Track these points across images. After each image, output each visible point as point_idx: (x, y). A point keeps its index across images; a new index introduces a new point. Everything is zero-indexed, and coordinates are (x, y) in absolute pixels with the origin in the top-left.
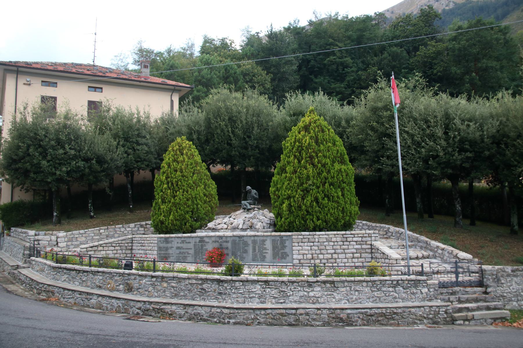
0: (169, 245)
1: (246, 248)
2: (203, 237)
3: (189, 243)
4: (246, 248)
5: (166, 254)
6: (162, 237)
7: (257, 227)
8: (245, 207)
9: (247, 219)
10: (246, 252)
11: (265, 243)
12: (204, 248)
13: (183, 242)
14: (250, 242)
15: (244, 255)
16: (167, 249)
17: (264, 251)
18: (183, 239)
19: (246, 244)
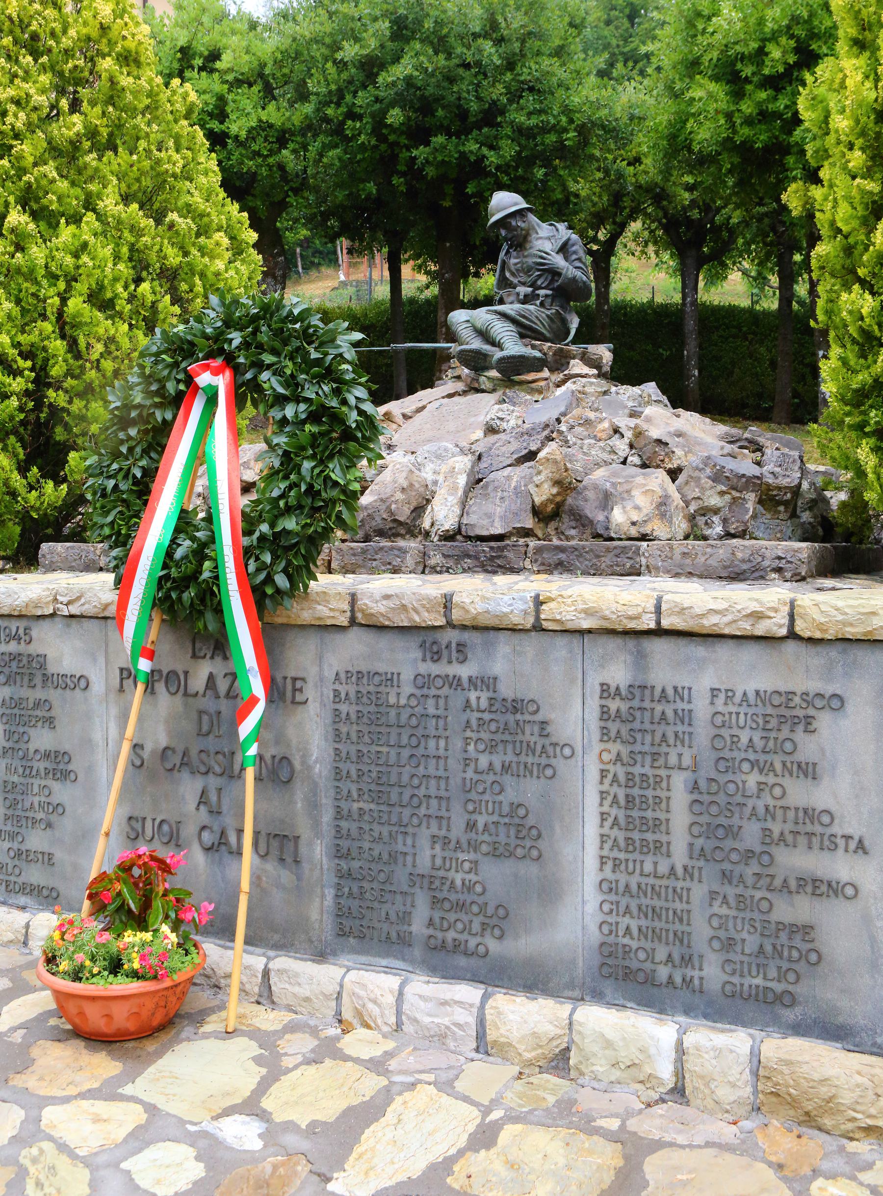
4: (528, 791)
7: (620, 517)
8: (476, 344)
9: (508, 447)
11: (808, 748)
12: (41, 739)
15: (496, 876)
17: (797, 860)
19: (517, 729)
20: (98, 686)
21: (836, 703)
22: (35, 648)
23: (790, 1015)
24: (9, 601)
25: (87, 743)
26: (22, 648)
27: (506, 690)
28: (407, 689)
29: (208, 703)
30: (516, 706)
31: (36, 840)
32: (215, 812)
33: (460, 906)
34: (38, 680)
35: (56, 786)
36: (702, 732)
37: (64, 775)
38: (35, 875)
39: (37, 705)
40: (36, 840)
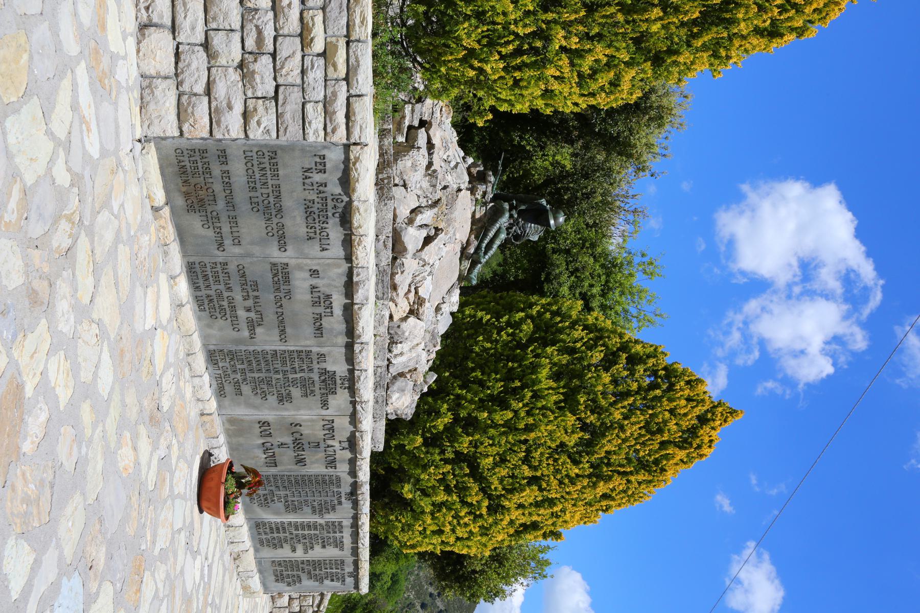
0: (296, 223)
1: (308, 510)
2: (352, 390)
3: (319, 331)
5: (231, 204)
6: (347, 181)
10: (291, 508)
12: (296, 392)
13: (322, 300)
14: (331, 517)
15: (280, 506)
16: (270, 208)
18: (338, 301)
20: (324, 412)
21: (342, 549)
22: (339, 390)
23: (258, 546)
24: (362, 387)
25: (299, 409)
26: (338, 386)
27: (337, 507)
28: (336, 490)
29: (322, 445)
30: (334, 509)
31: (246, 389)
32: (279, 446)
33: (266, 500)
34: (323, 391)
35: (275, 397)
36: (331, 535)
37: (281, 401)
38: (229, 388)
39: (312, 391)
40: (246, 389)
